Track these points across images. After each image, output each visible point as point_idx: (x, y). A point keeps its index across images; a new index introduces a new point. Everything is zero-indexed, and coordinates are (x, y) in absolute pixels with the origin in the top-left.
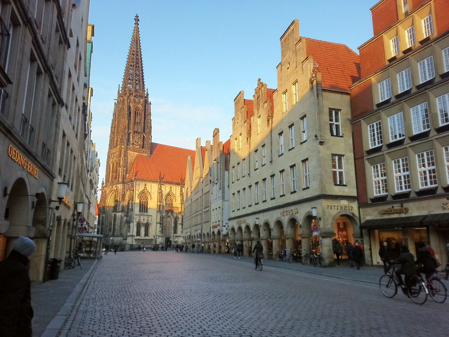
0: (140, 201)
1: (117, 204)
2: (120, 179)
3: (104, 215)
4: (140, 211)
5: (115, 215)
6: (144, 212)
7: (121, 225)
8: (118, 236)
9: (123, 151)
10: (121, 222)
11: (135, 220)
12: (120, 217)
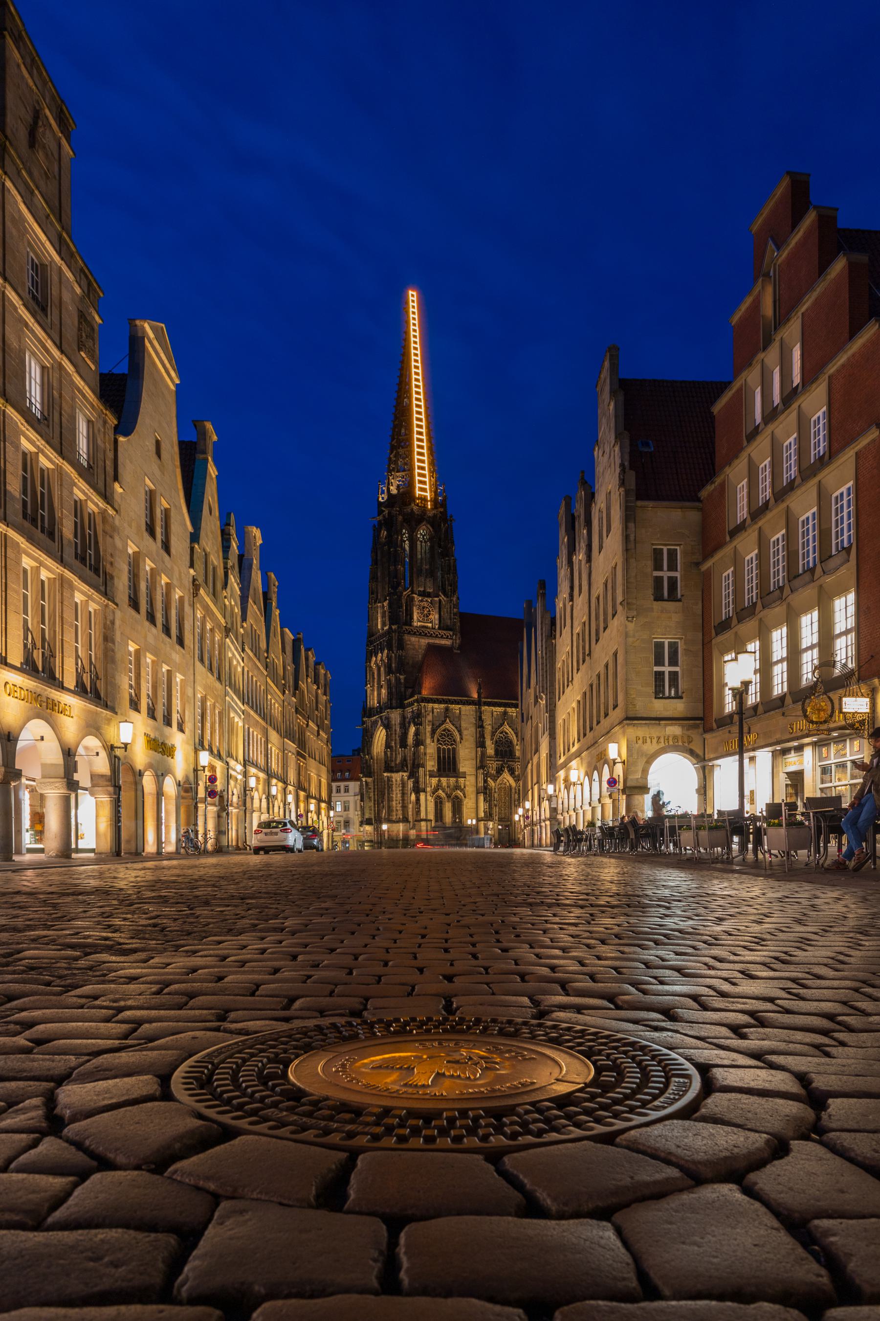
0: (439, 749)
1: (391, 757)
2: (394, 701)
3: (370, 780)
4: (439, 769)
5: (389, 779)
6: (449, 770)
7: (403, 800)
8: (398, 822)
9: (395, 636)
10: (403, 794)
11: (428, 789)
12: (399, 782)
